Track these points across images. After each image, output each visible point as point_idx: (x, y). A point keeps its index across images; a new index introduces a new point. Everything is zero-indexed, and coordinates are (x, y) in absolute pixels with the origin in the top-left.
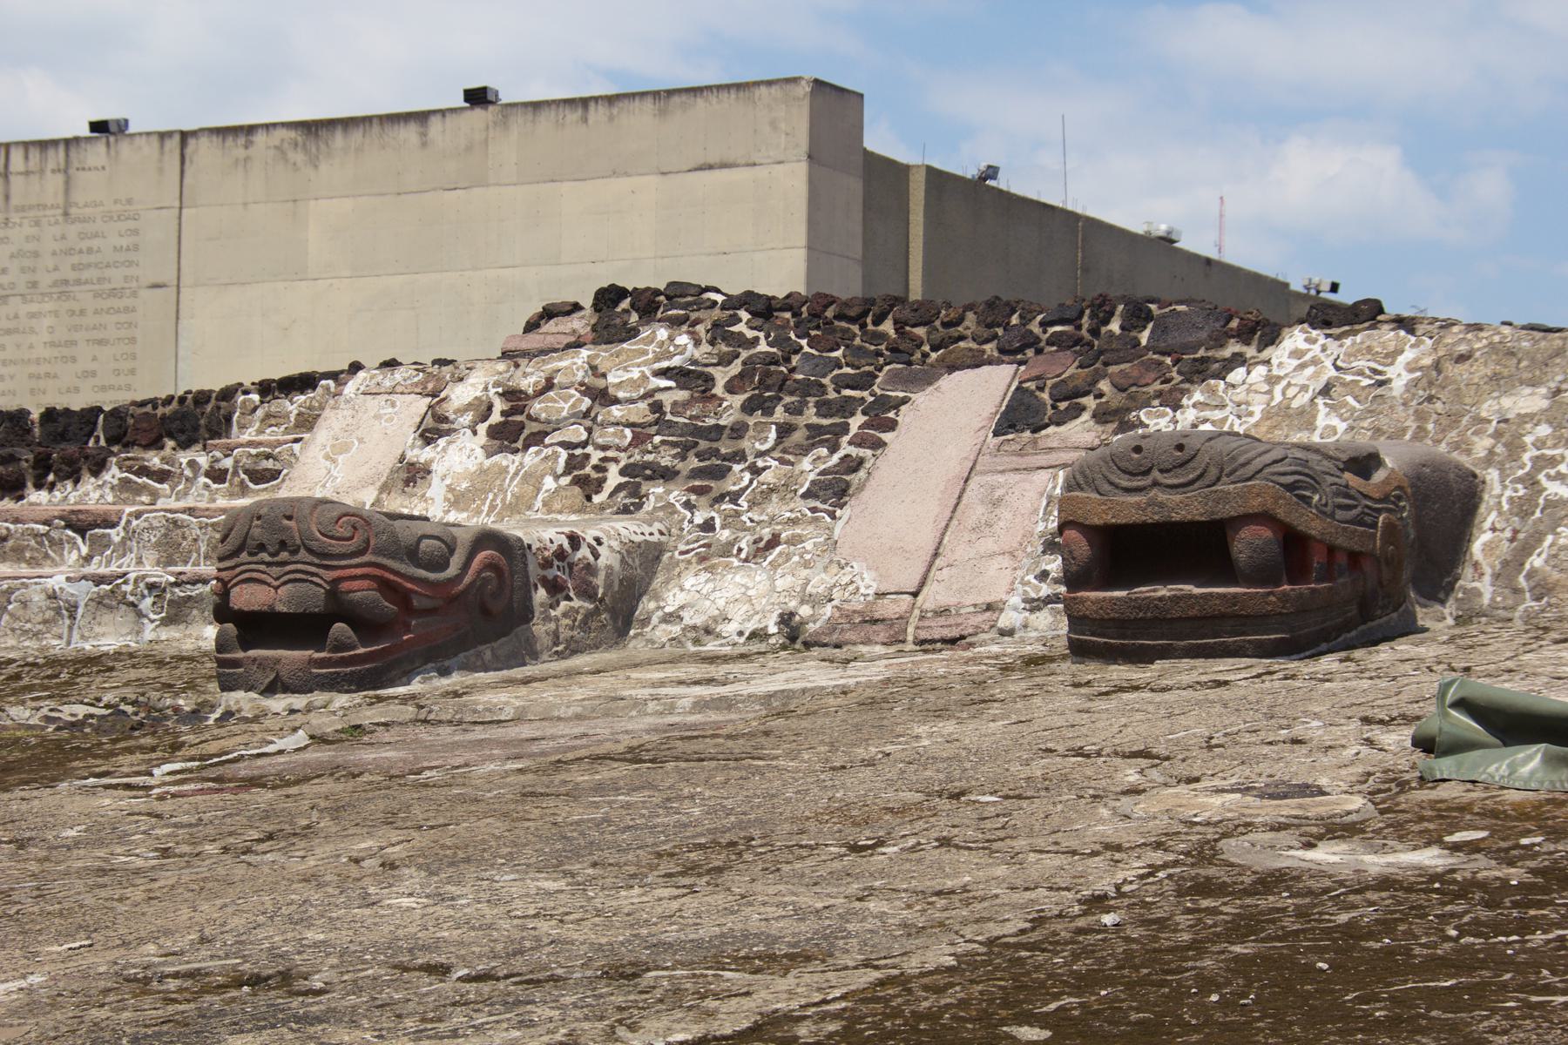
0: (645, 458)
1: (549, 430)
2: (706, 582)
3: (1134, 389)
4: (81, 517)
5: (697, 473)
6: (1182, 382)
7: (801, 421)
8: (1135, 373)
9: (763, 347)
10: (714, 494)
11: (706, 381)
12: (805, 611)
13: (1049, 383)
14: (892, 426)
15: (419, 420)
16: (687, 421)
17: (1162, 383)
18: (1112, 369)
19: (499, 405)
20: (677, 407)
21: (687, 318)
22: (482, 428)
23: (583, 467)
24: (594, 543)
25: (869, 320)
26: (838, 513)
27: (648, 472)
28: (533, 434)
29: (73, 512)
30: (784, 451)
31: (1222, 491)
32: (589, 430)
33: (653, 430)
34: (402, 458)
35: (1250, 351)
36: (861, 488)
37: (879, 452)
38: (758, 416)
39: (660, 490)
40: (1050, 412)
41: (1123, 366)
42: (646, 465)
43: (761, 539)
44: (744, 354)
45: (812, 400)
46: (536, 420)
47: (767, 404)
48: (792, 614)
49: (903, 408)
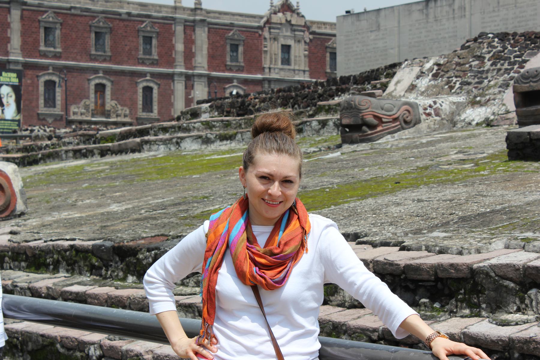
7: (504, 67)
9: (499, 48)
12: (492, 117)
19: (436, 68)
22: (431, 74)
26: (506, 91)
38: (494, 67)
42: (465, 82)
44: (494, 50)
48: (489, 118)
49: (528, 63)
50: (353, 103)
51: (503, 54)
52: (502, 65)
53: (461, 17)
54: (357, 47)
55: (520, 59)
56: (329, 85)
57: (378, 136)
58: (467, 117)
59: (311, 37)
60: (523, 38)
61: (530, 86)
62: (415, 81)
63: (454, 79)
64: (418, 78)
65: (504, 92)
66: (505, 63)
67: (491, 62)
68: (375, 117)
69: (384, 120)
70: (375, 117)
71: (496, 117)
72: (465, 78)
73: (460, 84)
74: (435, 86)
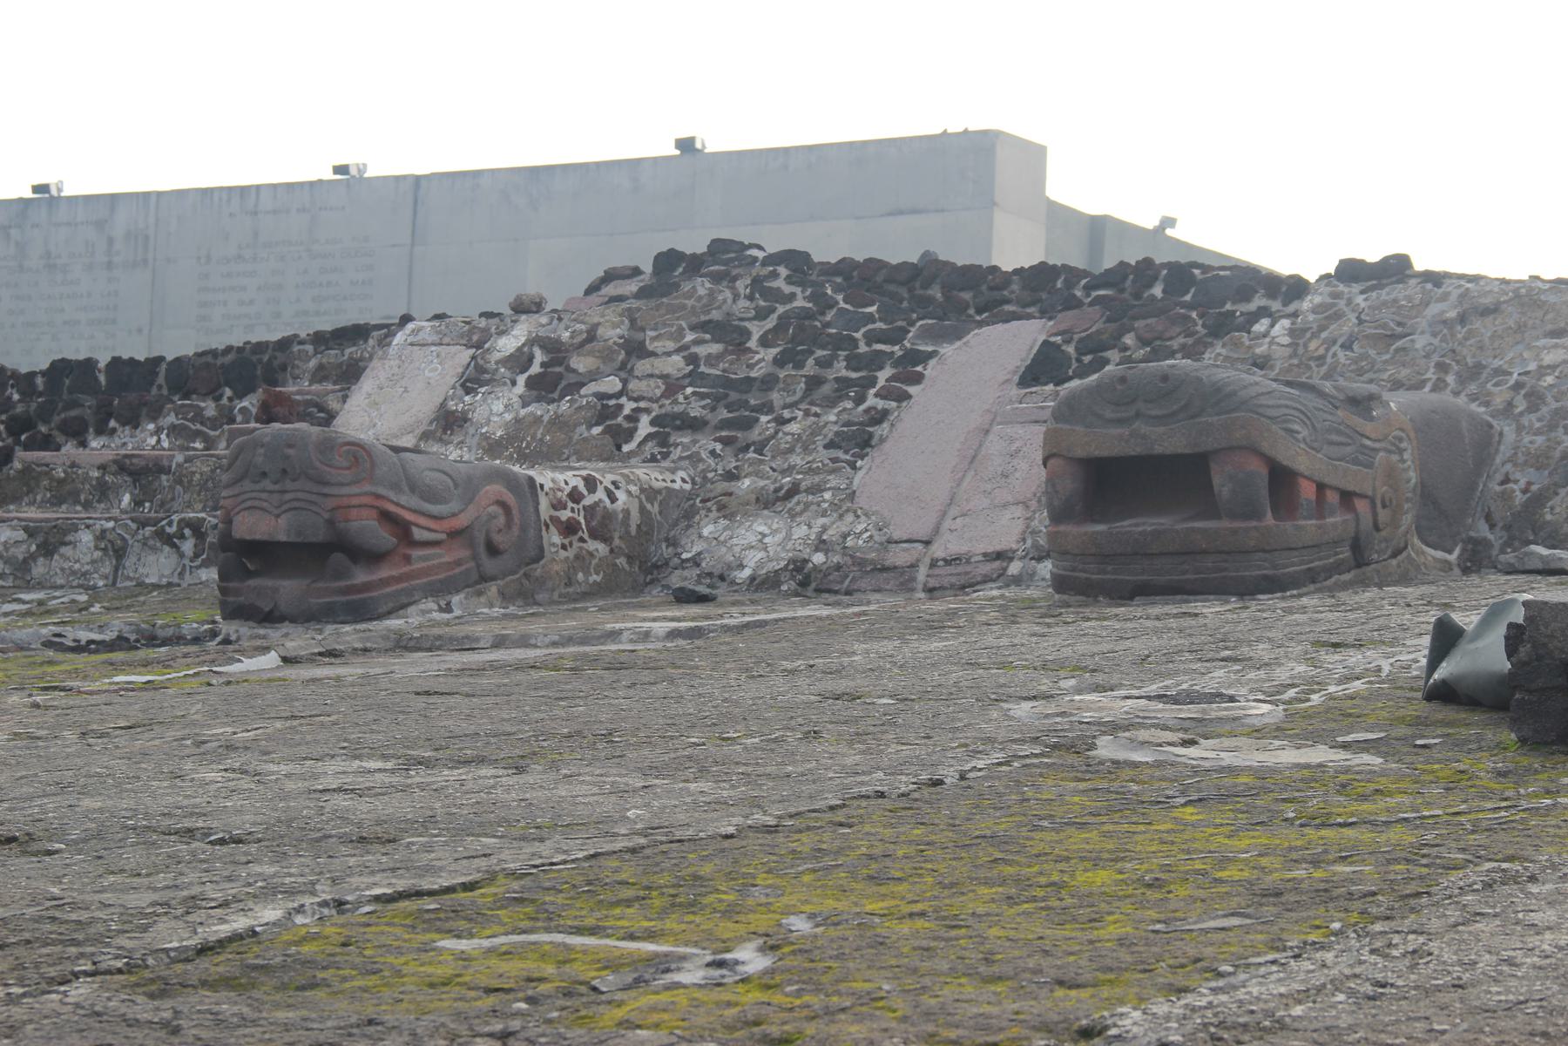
0: (676, 409)
1: (586, 381)
2: (725, 529)
4: (135, 461)
5: (725, 424)
6: (1205, 335)
7: (830, 374)
8: (1160, 328)
9: (800, 303)
10: (739, 445)
11: (741, 335)
12: (818, 558)
13: (1076, 337)
14: (918, 379)
15: (460, 370)
16: (719, 373)
18: (1139, 324)
19: (539, 356)
20: (711, 360)
22: (521, 380)
23: (616, 417)
24: (612, 487)
27: (678, 422)
28: (569, 385)
29: (126, 456)
30: (812, 403)
32: (625, 382)
33: (687, 381)
34: (443, 405)
36: (882, 440)
37: (904, 404)
39: (686, 440)
40: (1075, 365)
41: (1149, 321)
42: (675, 416)
43: (781, 488)
44: (781, 309)
45: (843, 353)
46: (574, 371)
47: (799, 358)
50: (291, 452)
52: (825, 363)
58: (708, 551)
65: (853, 466)
66: (834, 357)
67: (774, 351)
68: (386, 517)
69: (418, 534)
71: (836, 559)
72: (675, 402)
73: (652, 423)
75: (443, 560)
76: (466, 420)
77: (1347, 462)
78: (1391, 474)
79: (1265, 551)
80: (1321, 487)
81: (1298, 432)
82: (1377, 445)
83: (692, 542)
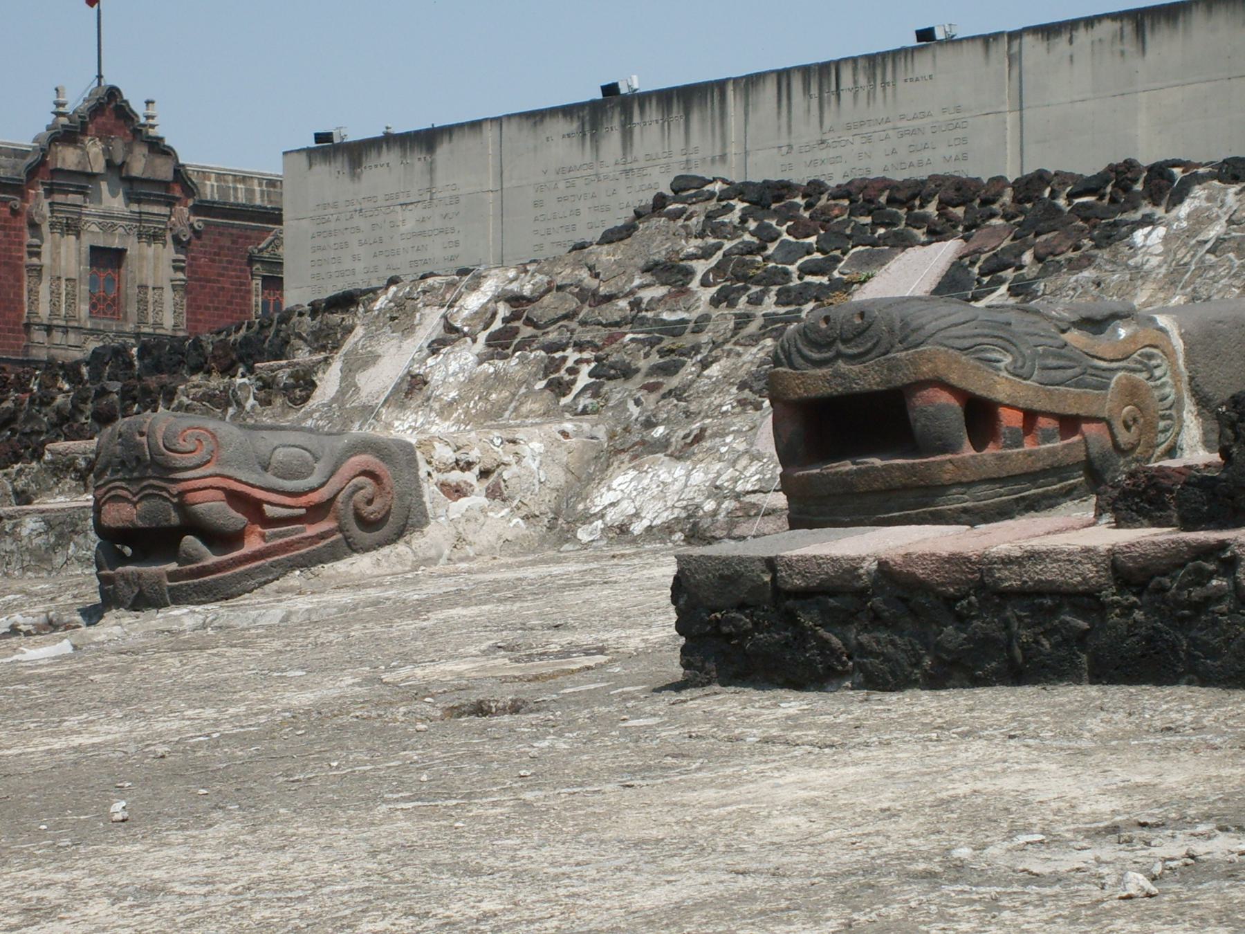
3: (1050, 258)
7: (760, 311)
13: (983, 257)
17: (1074, 250)
19: (503, 310)
20: (654, 303)
21: (683, 211)
22: (482, 337)
25: (917, 203)
27: (612, 372)
30: (736, 344)
31: (894, 358)
35: (1160, 212)
38: (723, 309)
44: (728, 245)
45: (775, 288)
47: (732, 296)
48: (698, 507)
51: (759, 258)
52: (756, 301)
53: (713, 161)
54: (355, 258)
55: (824, 280)
56: (96, 376)
57: (248, 575)
59: (197, 221)
60: (846, 202)
61: (836, 375)
62: (423, 361)
63: (572, 355)
64: (435, 347)
66: (764, 293)
67: (713, 290)
68: (236, 499)
70: (236, 499)
73: (591, 375)
74: (499, 379)
75: (305, 535)
76: (425, 383)
77: (1066, 386)
78: (1132, 393)
79: (960, 484)
80: (1030, 416)
81: (998, 361)
82: (1114, 365)
83: (601, 496)
